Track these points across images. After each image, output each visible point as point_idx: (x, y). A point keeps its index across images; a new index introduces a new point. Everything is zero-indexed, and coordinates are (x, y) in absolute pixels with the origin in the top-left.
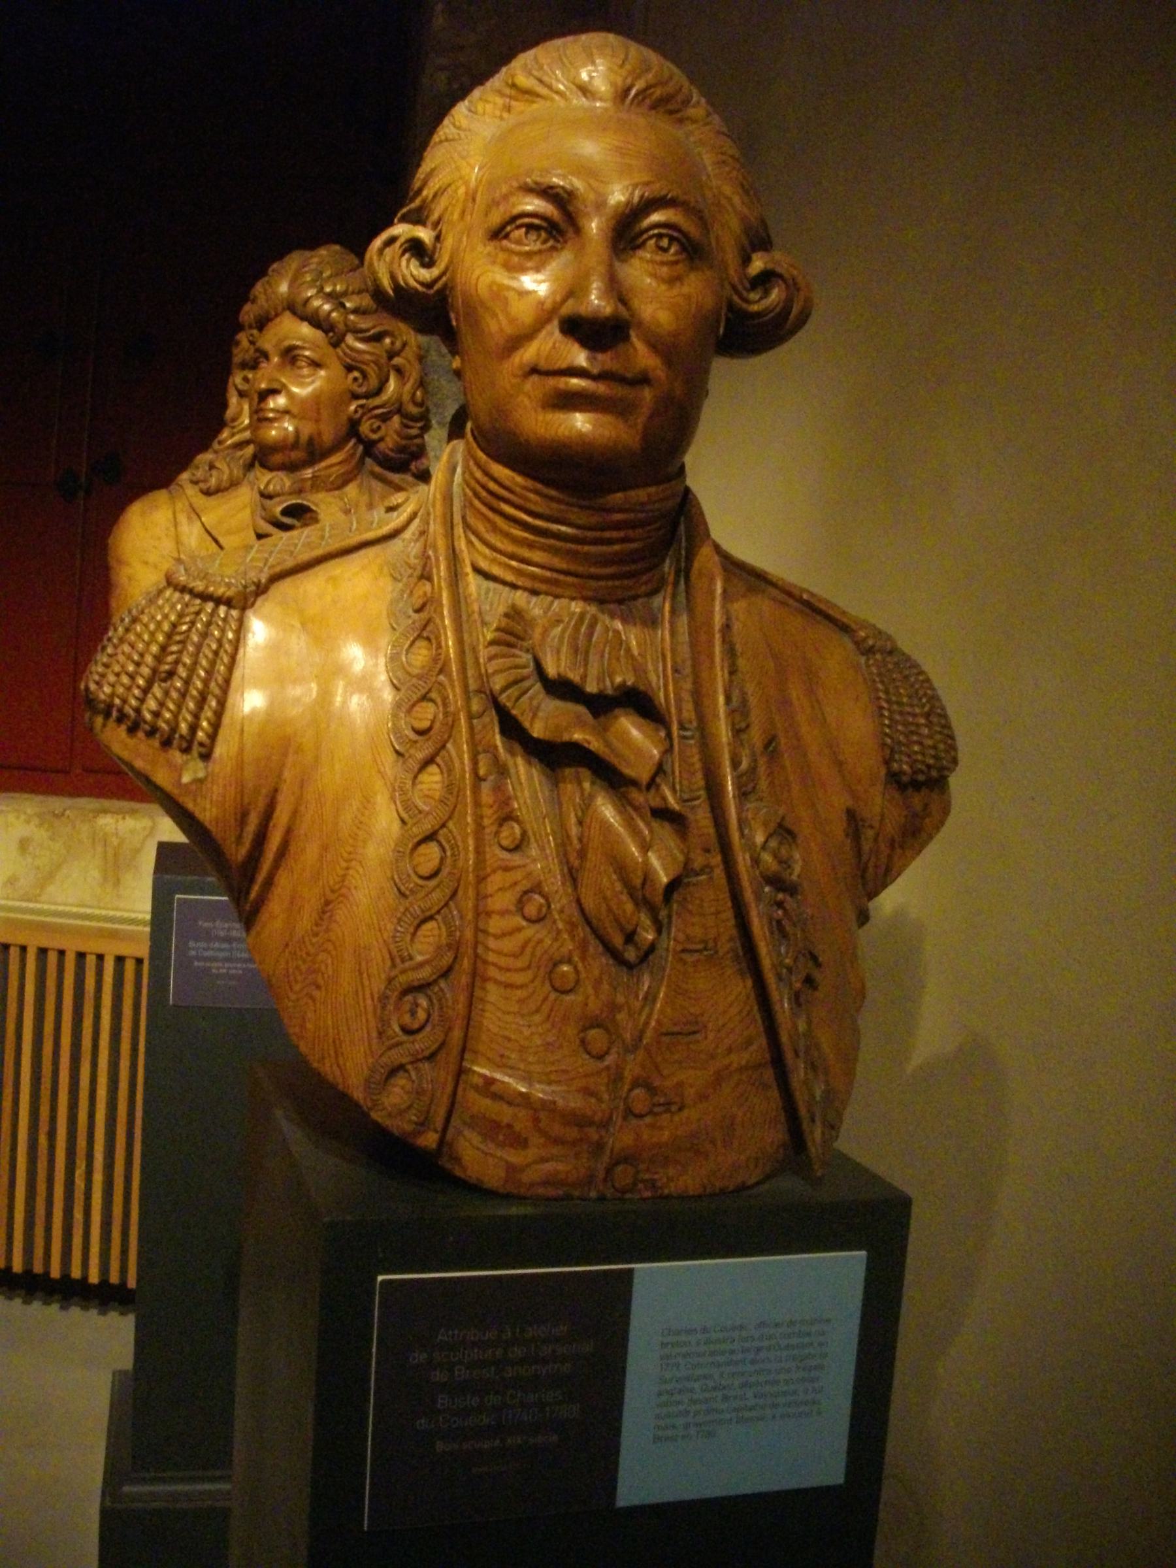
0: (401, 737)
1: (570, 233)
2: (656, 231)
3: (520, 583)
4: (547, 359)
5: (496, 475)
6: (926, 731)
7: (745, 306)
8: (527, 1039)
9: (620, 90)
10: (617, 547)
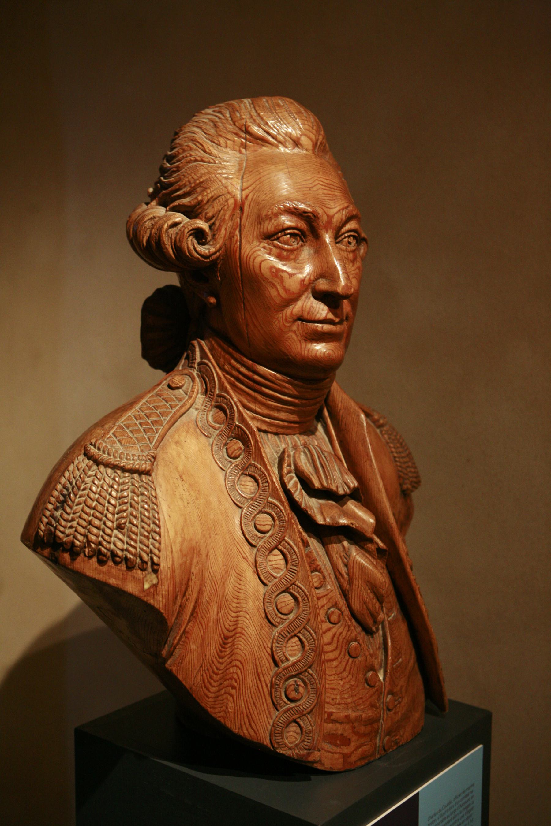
0: (253, 536)
1: (310, 237)
3: (270, 430)
4: (308, 313)
5: (261, 372)
8: (342, 686)
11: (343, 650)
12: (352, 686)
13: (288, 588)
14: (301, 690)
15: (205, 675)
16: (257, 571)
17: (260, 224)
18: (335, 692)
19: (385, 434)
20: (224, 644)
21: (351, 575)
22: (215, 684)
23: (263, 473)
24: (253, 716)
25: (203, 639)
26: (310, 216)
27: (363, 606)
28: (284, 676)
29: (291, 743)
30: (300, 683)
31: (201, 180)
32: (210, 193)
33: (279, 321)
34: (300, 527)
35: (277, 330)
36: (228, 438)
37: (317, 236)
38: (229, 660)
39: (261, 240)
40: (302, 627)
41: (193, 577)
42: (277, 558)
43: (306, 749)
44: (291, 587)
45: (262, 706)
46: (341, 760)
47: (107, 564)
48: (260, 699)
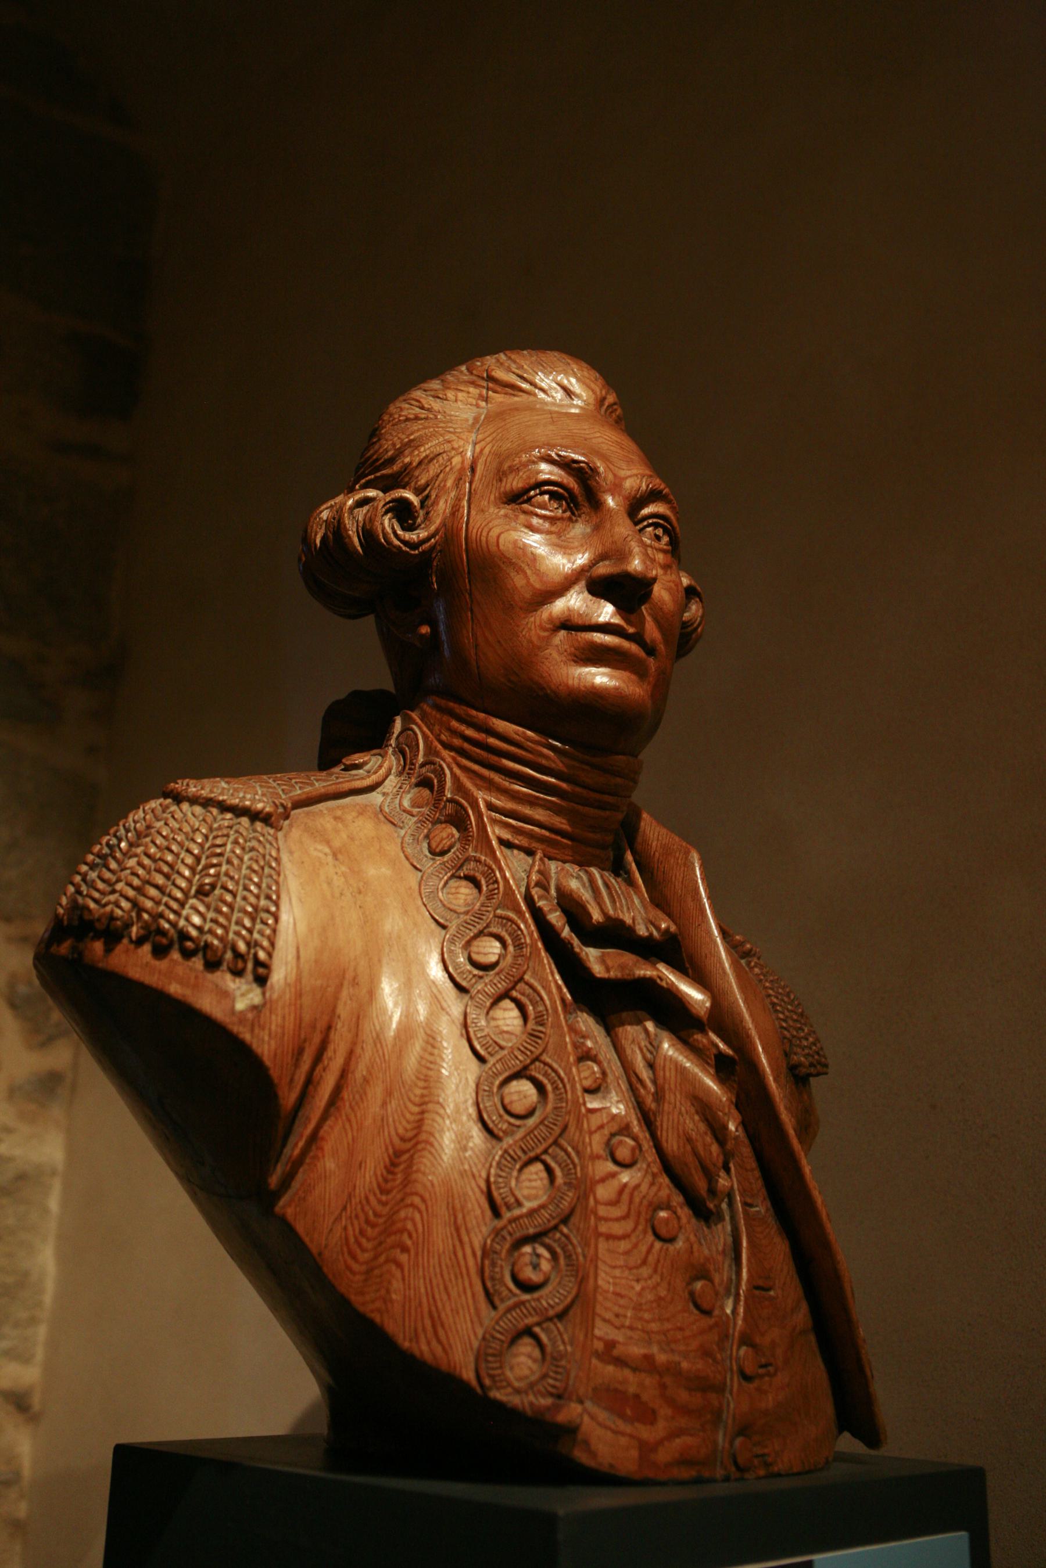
1: (586, 509)
3: (516, 842)
8: (640, 1294)
11: (642, 1220)
12: (660, 1298)
13: (526, 1068)
14: (545, 1266)
15: (350, 1228)
16: (467, 1033)
17: (501, 480)
18: (622, 1302)
19: (755, 966)
20: (392, 1166)
21: (660, 1081)
22: (369, 1245)
23: (490, 868)
24: (443, 1315)
25: (351, 1153)
26: (582, 468)
27: (684, 1147)
28: (510, 1234)
29: (520, 1379)
30: (545, 1253)
31: (412, 437)
32: (424, 451)
33: (530, 629)
34: (558, 977)
35: (525, 643)
36: (434, 823)
37: (596, 503)
38: (399, 1196)
40: (551, 1141)
41: (339, 1025)
42: (508, 1016)
43: (551, 1395)
44: (533, 1067)
45: (463, 1298)
46: (634, 1453)
47: (169, 957)
48: (460, 1280)
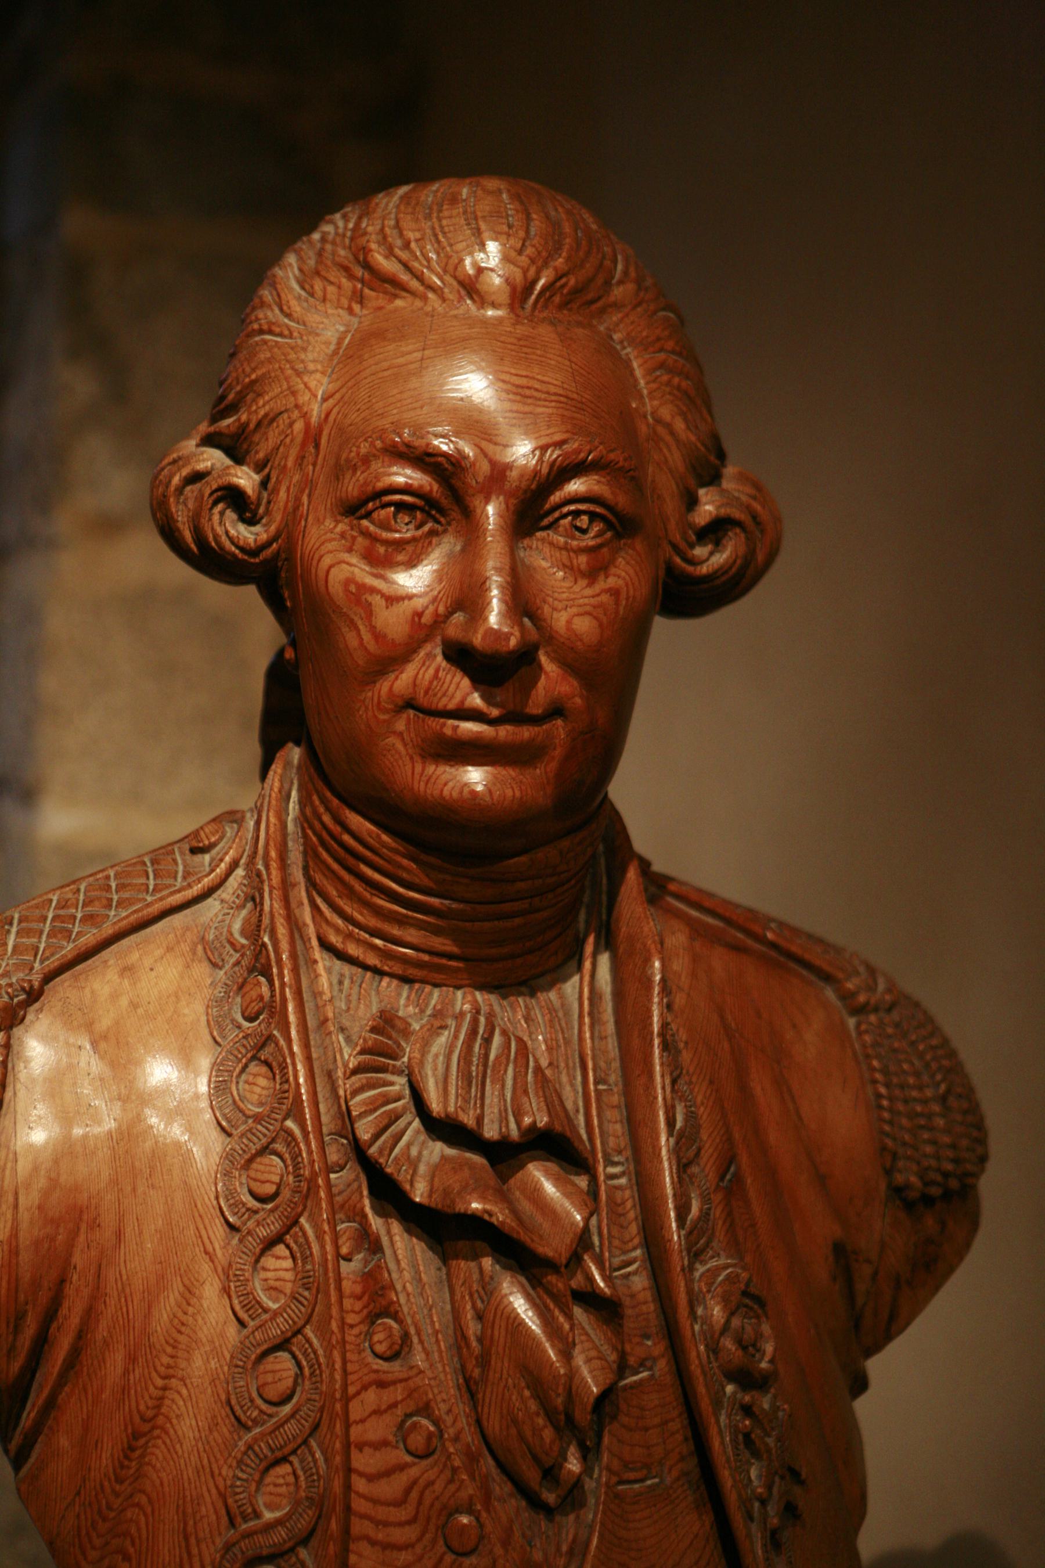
0: (235, 1205)
1: (455, 514)
2: (572, 508)
3: (386, 968)
4: (426, 692)
5: (354, 827)
6: (940, 1122)
7: (690, 569)
9: (519, 289)
10: (517, 921)
11: (432, 1527)
17: (338, 479)
31: (253, 377)
33: (367, 708)
35: (363, 727)
39: (339, 518)
41: (75, 1277)
